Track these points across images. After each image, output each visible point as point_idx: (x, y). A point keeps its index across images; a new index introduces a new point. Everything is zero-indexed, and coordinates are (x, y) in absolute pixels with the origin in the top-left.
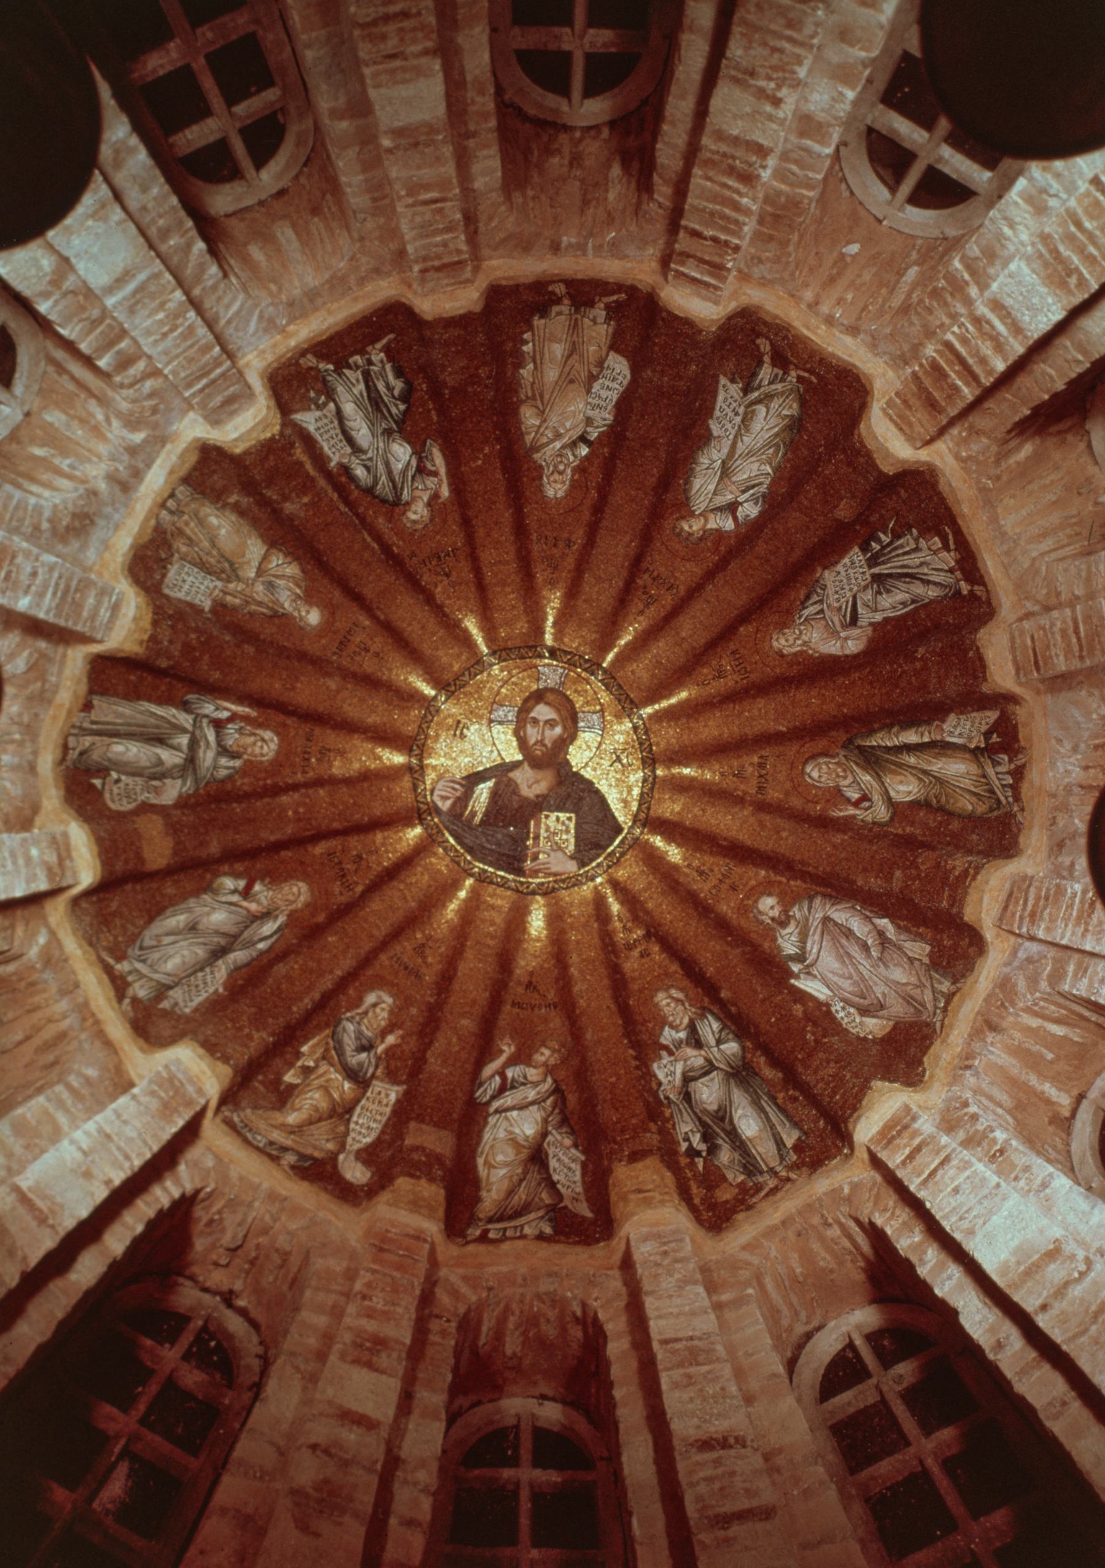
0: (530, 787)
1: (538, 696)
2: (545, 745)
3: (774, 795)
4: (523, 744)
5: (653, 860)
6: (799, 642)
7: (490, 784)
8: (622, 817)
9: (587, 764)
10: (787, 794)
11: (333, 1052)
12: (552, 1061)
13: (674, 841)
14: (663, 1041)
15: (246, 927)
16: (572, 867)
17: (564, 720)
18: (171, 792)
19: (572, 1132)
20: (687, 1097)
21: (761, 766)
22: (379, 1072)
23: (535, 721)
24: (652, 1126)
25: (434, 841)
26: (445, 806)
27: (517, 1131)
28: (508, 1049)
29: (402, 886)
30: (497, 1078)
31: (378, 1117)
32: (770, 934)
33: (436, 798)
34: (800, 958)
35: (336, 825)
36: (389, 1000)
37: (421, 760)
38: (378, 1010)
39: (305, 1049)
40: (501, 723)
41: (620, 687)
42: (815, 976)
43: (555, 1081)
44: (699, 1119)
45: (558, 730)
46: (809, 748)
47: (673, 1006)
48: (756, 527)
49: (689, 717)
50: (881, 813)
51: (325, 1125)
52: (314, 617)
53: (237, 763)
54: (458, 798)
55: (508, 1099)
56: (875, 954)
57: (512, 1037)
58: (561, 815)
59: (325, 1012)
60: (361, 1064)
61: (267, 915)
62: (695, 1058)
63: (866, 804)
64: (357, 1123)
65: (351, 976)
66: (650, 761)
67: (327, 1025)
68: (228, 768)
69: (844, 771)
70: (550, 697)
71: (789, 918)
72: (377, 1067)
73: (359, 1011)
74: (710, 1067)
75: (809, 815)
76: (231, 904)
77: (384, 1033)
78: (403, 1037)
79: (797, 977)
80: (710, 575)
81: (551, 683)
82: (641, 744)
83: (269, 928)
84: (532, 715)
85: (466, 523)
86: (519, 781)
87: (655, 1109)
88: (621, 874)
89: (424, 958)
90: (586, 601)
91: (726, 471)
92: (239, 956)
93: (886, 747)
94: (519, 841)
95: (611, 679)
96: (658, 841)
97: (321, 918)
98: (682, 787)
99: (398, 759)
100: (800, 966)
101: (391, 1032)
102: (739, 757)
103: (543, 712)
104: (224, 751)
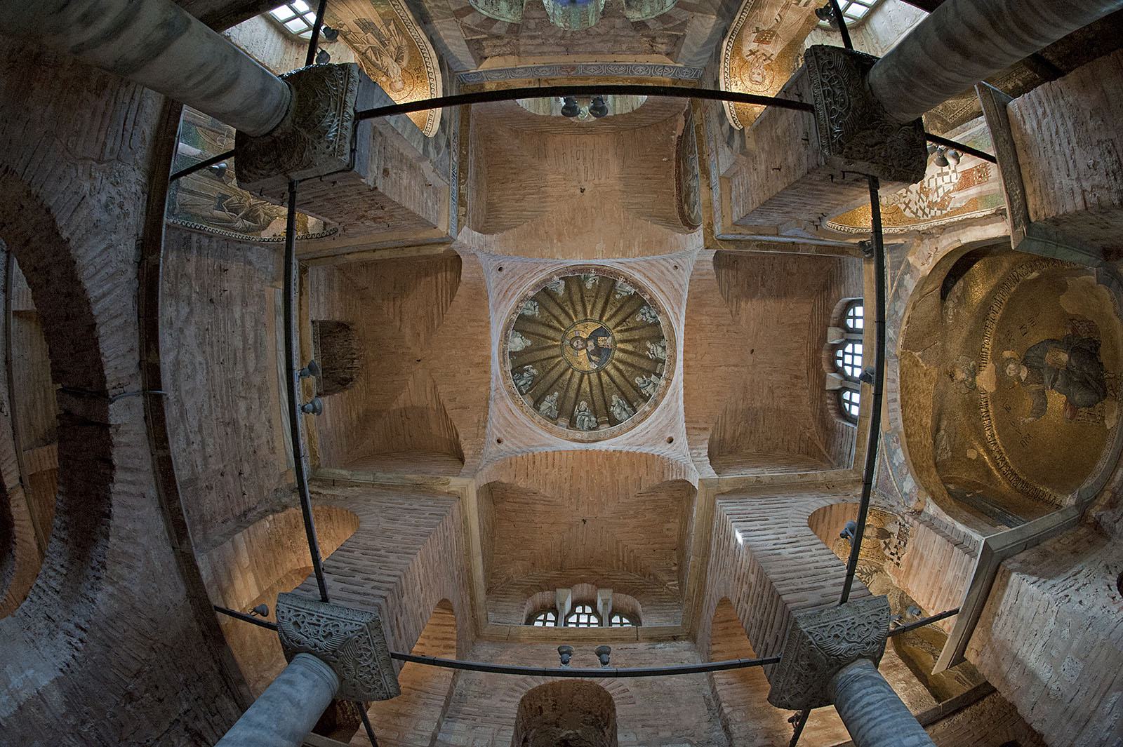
5: (608, 320)
16: (610, 338)
18: (593, 419)
32: (623, 297)
48: (538, 302)
52: (556, 393)
59: (636, 388)
62: (648, 315)
65: (632, 386)
66: (586, 320)
80: (547, 310)
85: (536, 362)
91: (529, 309)
95: (568, 329)
96: (604, 318)
98: (592, 313)
99: (586, 376)
103: (575, 344)
104: (585, 411)
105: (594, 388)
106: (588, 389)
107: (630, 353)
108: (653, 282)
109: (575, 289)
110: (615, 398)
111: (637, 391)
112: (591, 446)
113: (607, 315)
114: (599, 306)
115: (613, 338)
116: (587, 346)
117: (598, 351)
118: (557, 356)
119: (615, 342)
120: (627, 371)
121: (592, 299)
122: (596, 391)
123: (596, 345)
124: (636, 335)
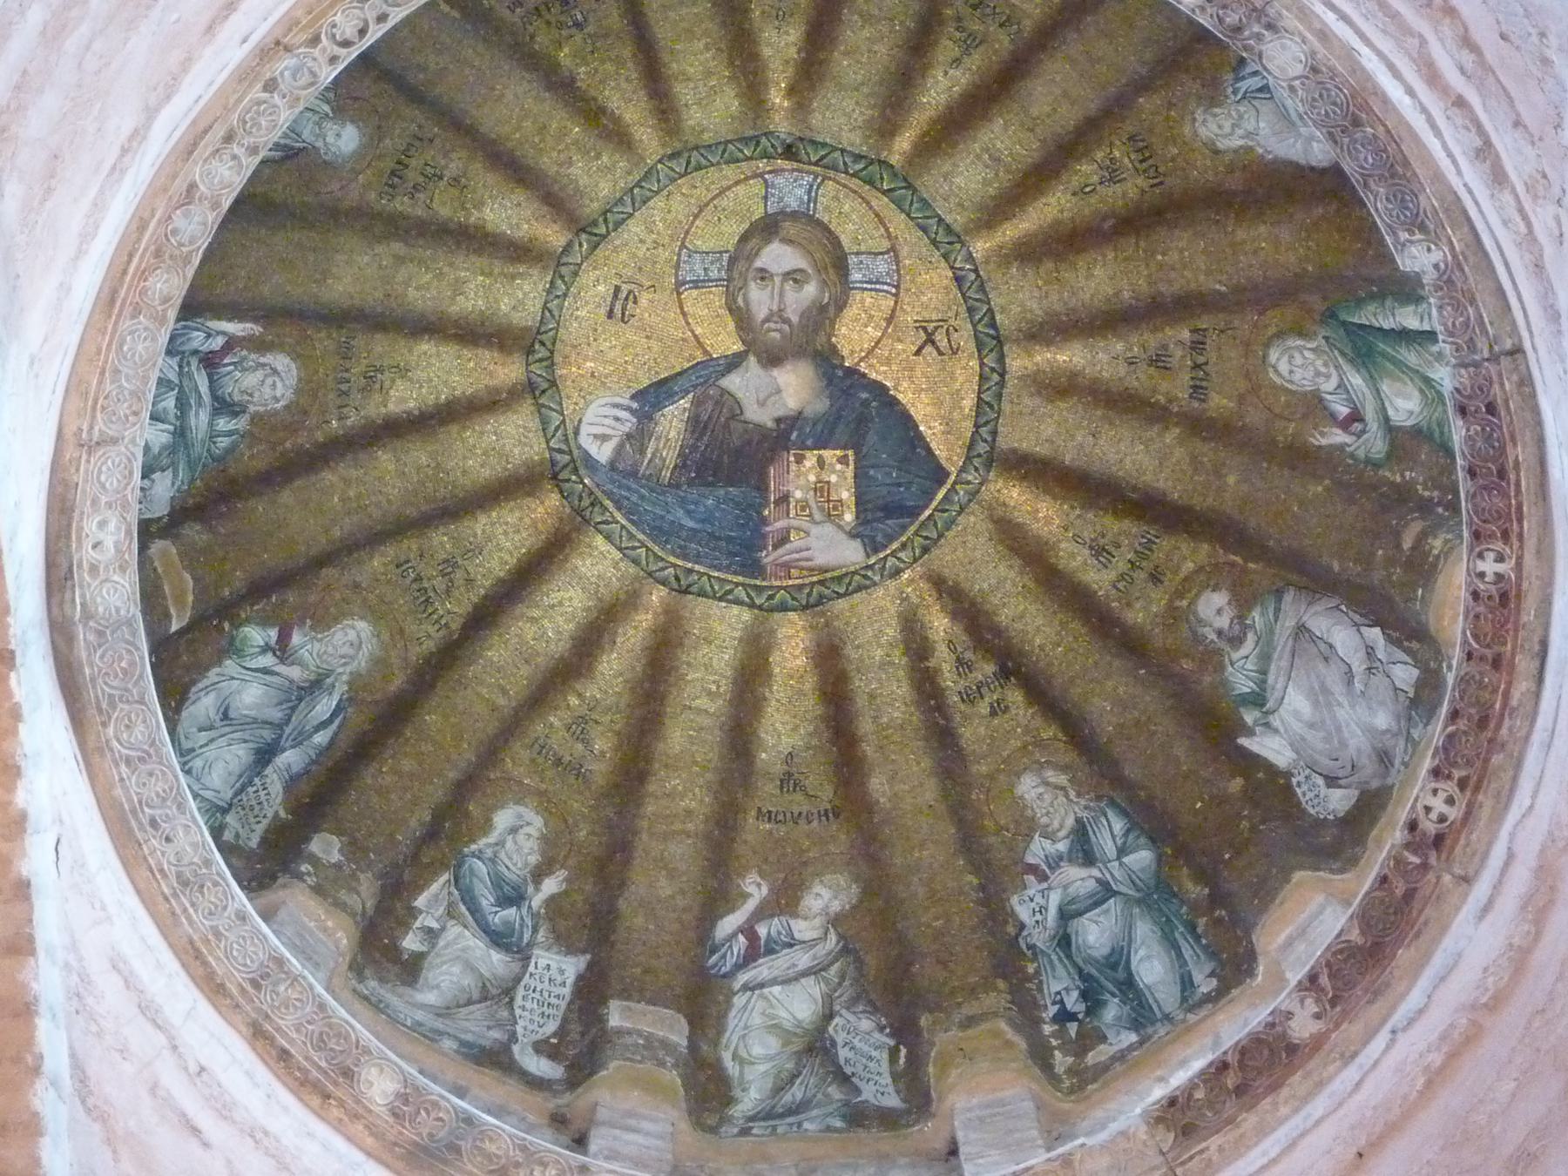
1: (767, 228)
2: (787, 321)
3: (1219, 403)
4: (743, 319)
6: (1240, 132)
7: (684, 403)
8: (945, 448)
9: (870, 352)
10: (1241, 399)
11: (463, 908)
12: (836, 906)
13: (1047, 491)
14: (1030, 860)
15: (293, 709)
16: (851, 554)
19: (874, 1009)
20: (1064, 941)
21: (1197, 346)
22: (541, 937)
23: (764, 275)
24: (1001, 984)
25: (587, 521)
26: (602, 453)
27: (783, 1014)
28: (755, 889)
29: (536, 613)
30: (741, 938)
31: (554, 1001)
32: (1212, 659)
33: (586, 441)
34: (1257, 699)
35: (411, 512)
36: (538, 821)
37: (551, 366)
38: (521, 837)
39: (421, 902)
40: (696, 284)
41: (925, 204)
42: (1276, 731)
43: (841, 937)
44: (1080, 971)
45: (811, 290)
46: (1274, 319)
47: (1047, 797)
49: (1059, 257)
50: (1374, 443)
51: (478, 1010)
53: (241, 423)
54: (629, 436)
55: (763, 969)
56: (1358, 686)
57: (762, 874)
58: (827, 454)
60: (507, 923)
61: (316, 685)
62: (1079, 879)
63: (1357, 426)
64: (523, 1008)
65: (467, 785)
66: (992, 341)
67: (444, 866)
68: (230, 433)
69: (1326, 365)
71: (1245, 629)
72: (535, 930)
73: (491, 839)
74: (1106, 891)
75: (1274, 442)
76: (266, 671)
77: (538, 875)
78: (567, 880)
79: (1250, 733)
82: (971, 310)
83: (325, 706)
84: (758, 264)
86: (740, 395)
87: (1009, 961)
88: (946, 558)
89: (587, 743)
90: (846, 54)
92: (291, 758)
93: (1380, 329)
96: (1014, 495)
97: (398, 682)
100: (1257, 714)
101: (550, 873)
102: (1155, 330)
103: (778, 256)
104: (224, 406)
105: (418, 454)
106: (402, 398)
107: (740, 736)
108: (1435, 1079)
109: (1270, 245)
110: (346, 646)
111: (432, 834)
112: (34, 683)
113: (1043, 514)
114: (1129, 453)
115: (852, 582)
116: (772, 359)
117: (734, 460)
118: (665, 109)
119: (821, 592)
120: (580, 728)
121: (1177, 388)
122: (391, 476)
123: (787, 435)
124: (901, 779)
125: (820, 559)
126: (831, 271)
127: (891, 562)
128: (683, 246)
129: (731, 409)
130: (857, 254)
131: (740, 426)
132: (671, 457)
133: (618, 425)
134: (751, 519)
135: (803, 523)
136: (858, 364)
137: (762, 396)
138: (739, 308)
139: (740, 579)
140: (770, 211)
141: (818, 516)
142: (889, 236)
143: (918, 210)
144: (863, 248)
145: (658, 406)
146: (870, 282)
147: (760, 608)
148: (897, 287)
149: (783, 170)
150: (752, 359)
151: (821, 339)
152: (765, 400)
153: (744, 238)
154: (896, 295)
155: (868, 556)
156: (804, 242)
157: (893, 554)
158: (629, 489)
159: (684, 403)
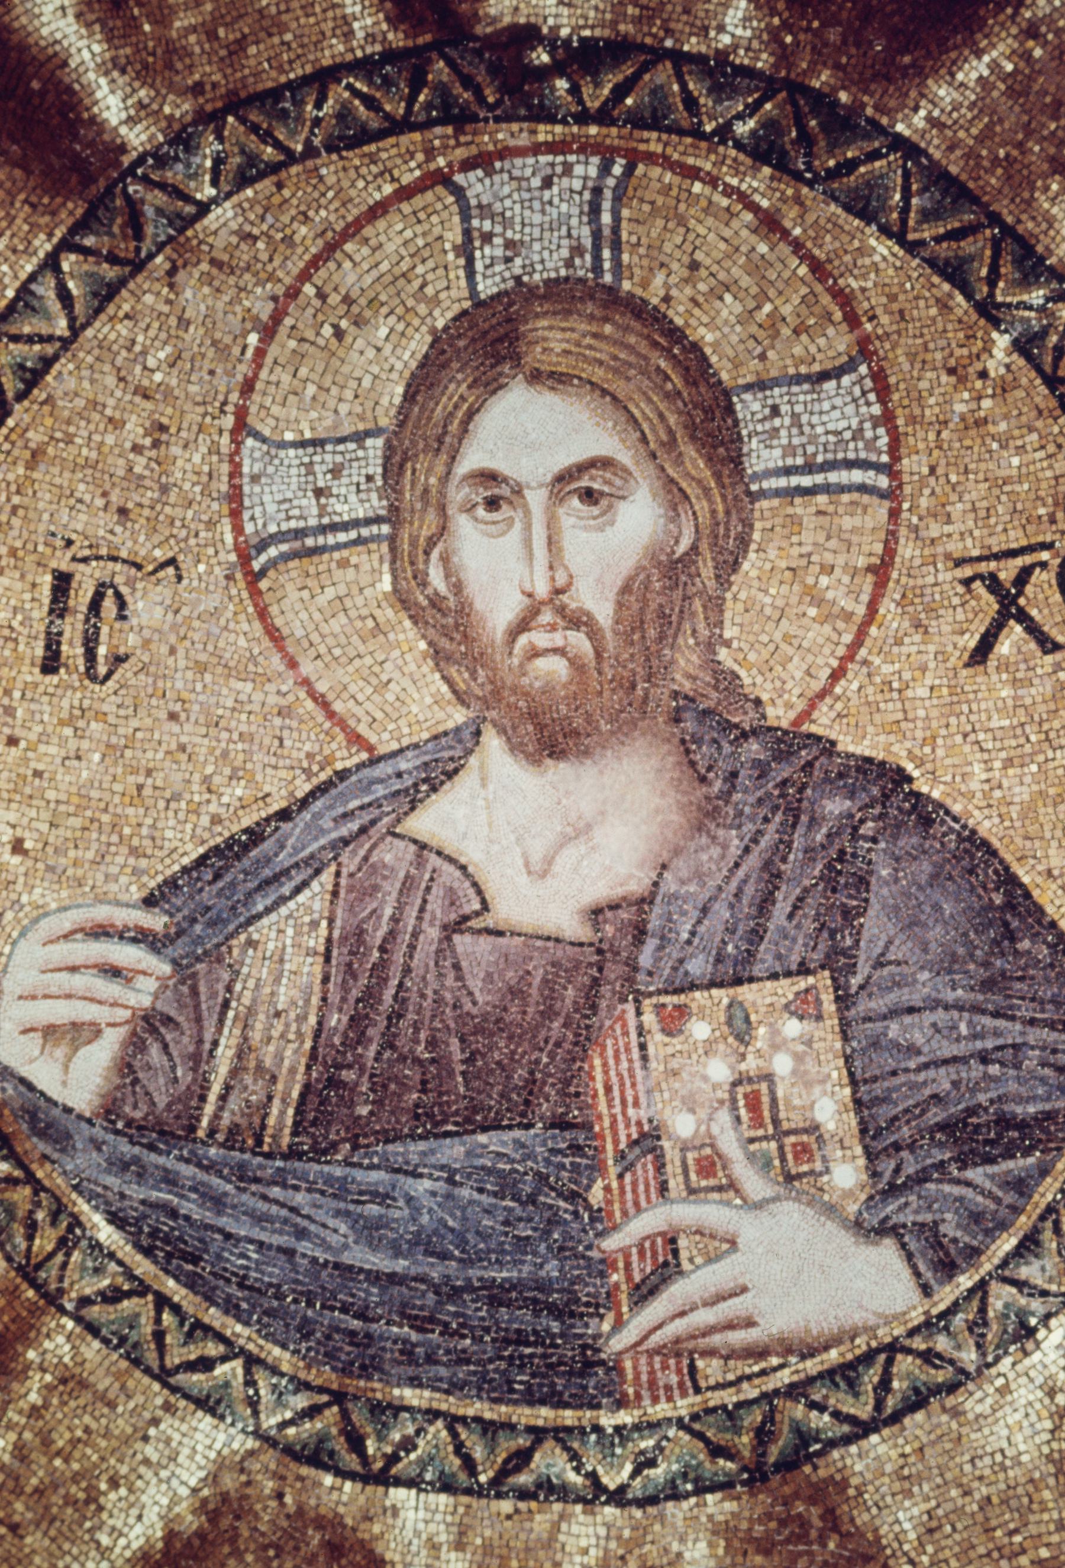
0: (541, 871)
2: (578, 620)
4: (448, 626)
16: (874, 1288)
17: (658, 451)
23: (496, 492)
40: (304, 546)
45: (638, 520)
54: (150, 1024)
70: (552, 338)
81: (547, 261)
86: (472, 854)
94: (554, 1201)
103: (527, 429)
125: (779, 1315)
126: (689, 451)
127: (1001, 1296)
128: (241, 427)
129: (452, 899)
130: (761, 385)
131: (485, 943)
132: (289, 1059)
133: (111, 989)
134: (554, 1221)
135: (712, 1213)
136: (806, 715)
137: (537, 850)
138: (436, 602)
139: (544, 1415)
140: (486, 288)
141: (755, 1185)
142: (852, 320)
143: (927, 216)
144: (777, 362)
145: (235, 918)
146: (809, 468)
147: (619, 1497)
148: (890, 470)
149: (505, 153)
150: (492, 742)
151: (685, 663)
152: (549, 861)
153: (422, 382)
154: (892, 495)
155: (926, 1290)
156: (598, 374)
157: (1004, 1274)
158: (170, 1180)
159: (314, 899)
